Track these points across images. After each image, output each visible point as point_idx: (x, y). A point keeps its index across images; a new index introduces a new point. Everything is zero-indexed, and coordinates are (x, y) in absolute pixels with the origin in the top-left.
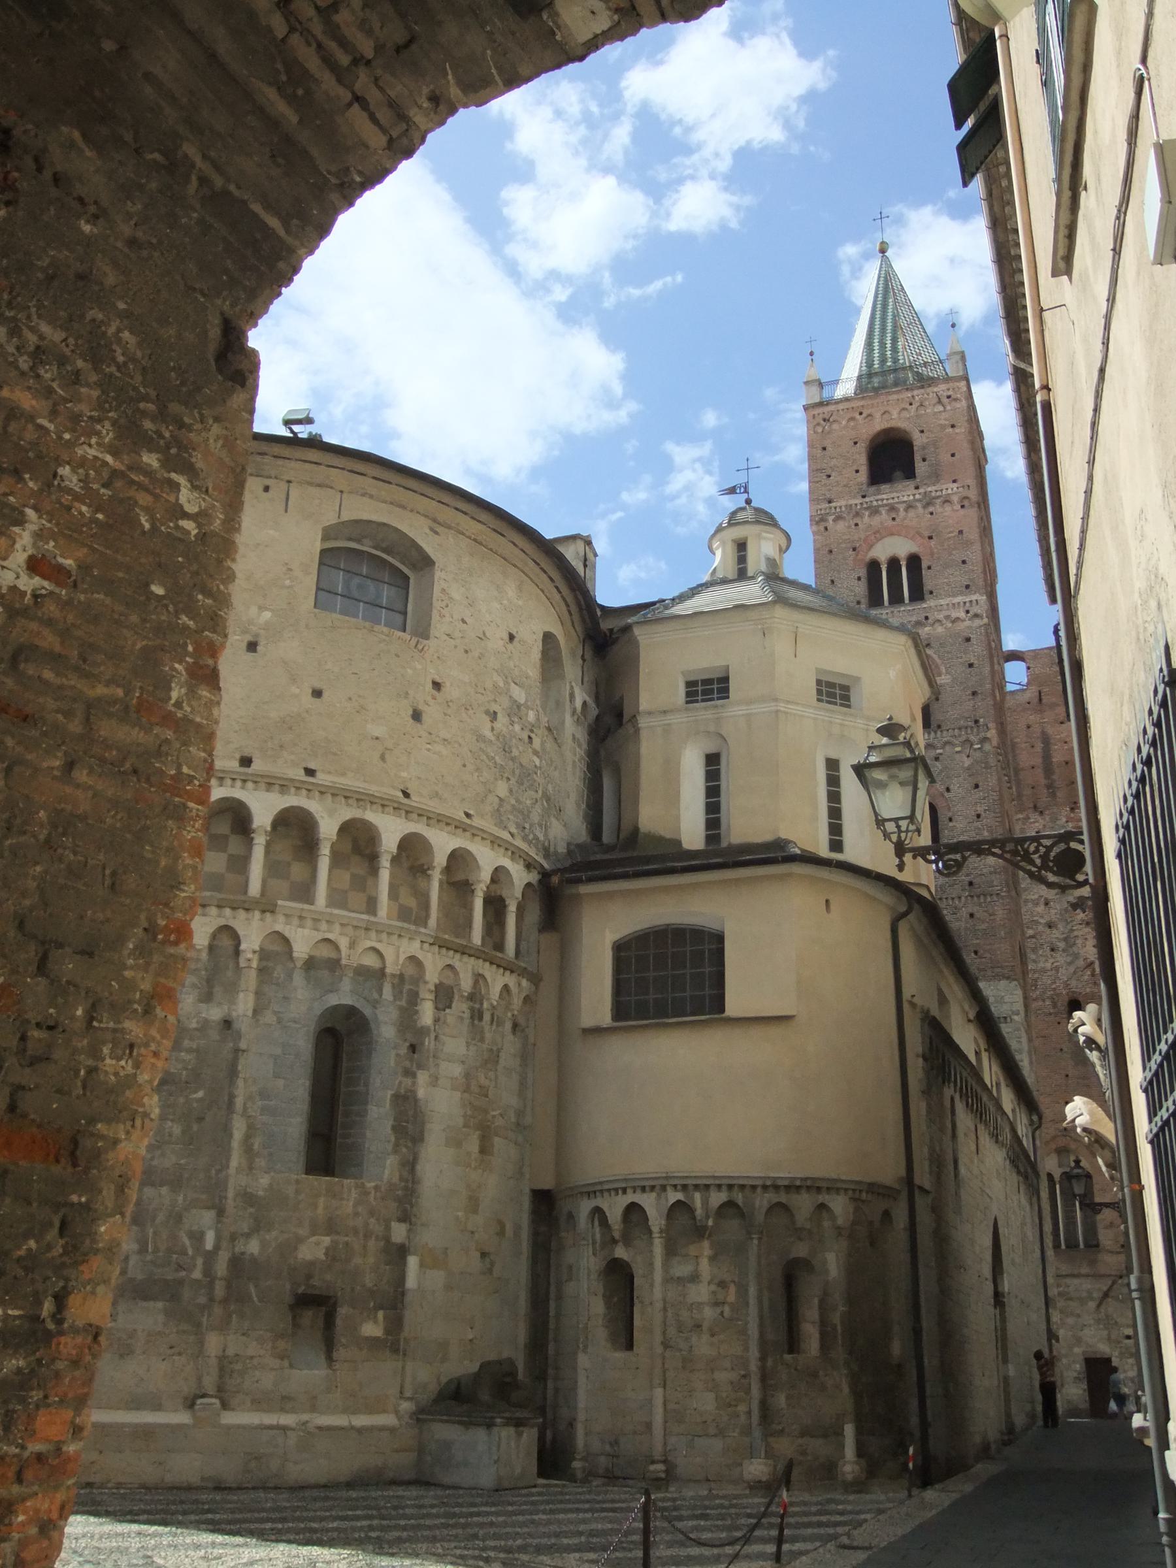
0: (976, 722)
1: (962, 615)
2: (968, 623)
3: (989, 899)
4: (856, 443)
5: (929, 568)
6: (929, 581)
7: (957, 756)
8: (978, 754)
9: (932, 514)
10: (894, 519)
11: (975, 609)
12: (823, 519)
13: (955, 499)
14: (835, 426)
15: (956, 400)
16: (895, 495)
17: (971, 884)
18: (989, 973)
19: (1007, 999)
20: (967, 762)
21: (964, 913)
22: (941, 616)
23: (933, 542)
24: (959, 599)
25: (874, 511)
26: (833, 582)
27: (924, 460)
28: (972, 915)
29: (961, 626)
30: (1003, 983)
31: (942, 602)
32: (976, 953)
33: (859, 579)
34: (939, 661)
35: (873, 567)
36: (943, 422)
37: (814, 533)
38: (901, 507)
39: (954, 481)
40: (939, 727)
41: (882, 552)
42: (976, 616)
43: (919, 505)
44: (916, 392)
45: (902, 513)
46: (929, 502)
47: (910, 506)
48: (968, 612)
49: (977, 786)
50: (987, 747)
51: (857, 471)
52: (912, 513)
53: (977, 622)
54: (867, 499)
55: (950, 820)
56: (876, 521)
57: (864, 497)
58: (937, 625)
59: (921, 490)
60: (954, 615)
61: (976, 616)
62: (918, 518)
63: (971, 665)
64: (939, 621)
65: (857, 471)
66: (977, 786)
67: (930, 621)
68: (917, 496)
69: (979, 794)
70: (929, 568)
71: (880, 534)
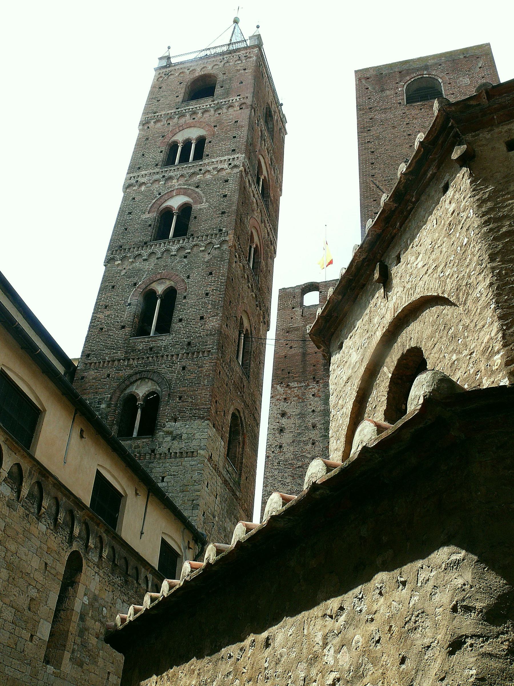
0: (221, 230)
1: (226, 166)
2: (229, 171)
3: (201, 355)
4: (180, 83)
5: (210, 142)
6: (207, 150)
7: (201, 254)
8: (216, 252)
9: (220, 114)
10: (194, 119)
11: (236, 162)
12: (148, 123)
13: (237, 104)
14: (171, 77)
15: (250, 57)
16: (198, 106)
17: (189, 344)
18: (188, 414)
19: (197, 436)
20: (207, 257)
21: (178, 366)
22: (210, 168)
23: (216, 128)
24: (226, 158)
25: (184, 115)
26: (143, 155)
27: (222, 87)
28: (184, 368)
29: (224, 173)
30: (198, 422)
31: (213, 160)
32: (180, 398)
33: (161, 152)
34: (203, 195)
35: (174, 147)
36: (239, 68)
37: (140, 130)
38: (200, 112)
39: (239, 95)
40: (192, 235)
41: (180, 138)
42: (236, 166)
43: (212, 109)
44: (225, 56)
45: (200, 115)
46: (218, 108)
47: (206, 111)
48: (230, 164)
49: (211, 274)
50: (225, 247)
51: (177, 97)
52: (206, 115)
53: (236, 170)
54: (179, 110)
55: (185, 298)
56: (182, 121)
57: (177, 109)
58: (207, 173)
59: (216, 102)
60: (220, 167)
61: (236, 166)
62: (211, 116)
63: (225, 196)
64: (209, 171)
65: (177, 97)
66: (211, 274)
67: (202, 172)
68: (212, 105)
69: (211, 278)
70: (210, 142)
71: (181, 128)
